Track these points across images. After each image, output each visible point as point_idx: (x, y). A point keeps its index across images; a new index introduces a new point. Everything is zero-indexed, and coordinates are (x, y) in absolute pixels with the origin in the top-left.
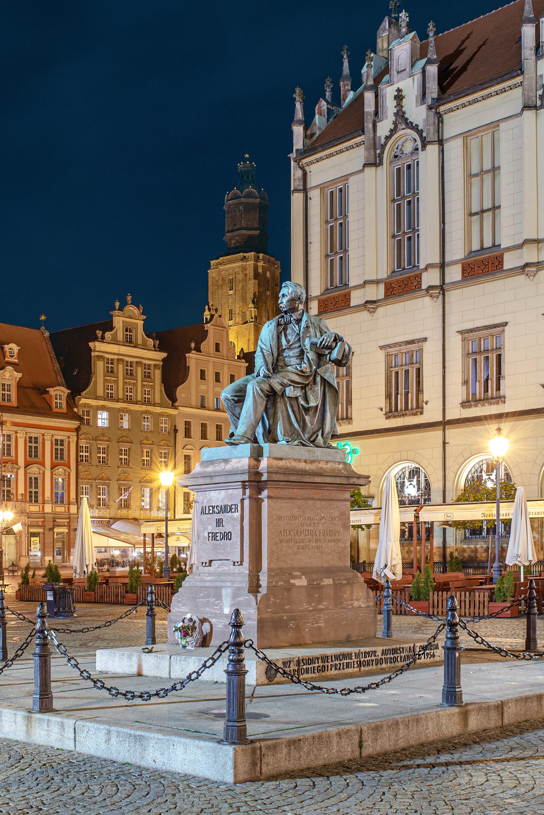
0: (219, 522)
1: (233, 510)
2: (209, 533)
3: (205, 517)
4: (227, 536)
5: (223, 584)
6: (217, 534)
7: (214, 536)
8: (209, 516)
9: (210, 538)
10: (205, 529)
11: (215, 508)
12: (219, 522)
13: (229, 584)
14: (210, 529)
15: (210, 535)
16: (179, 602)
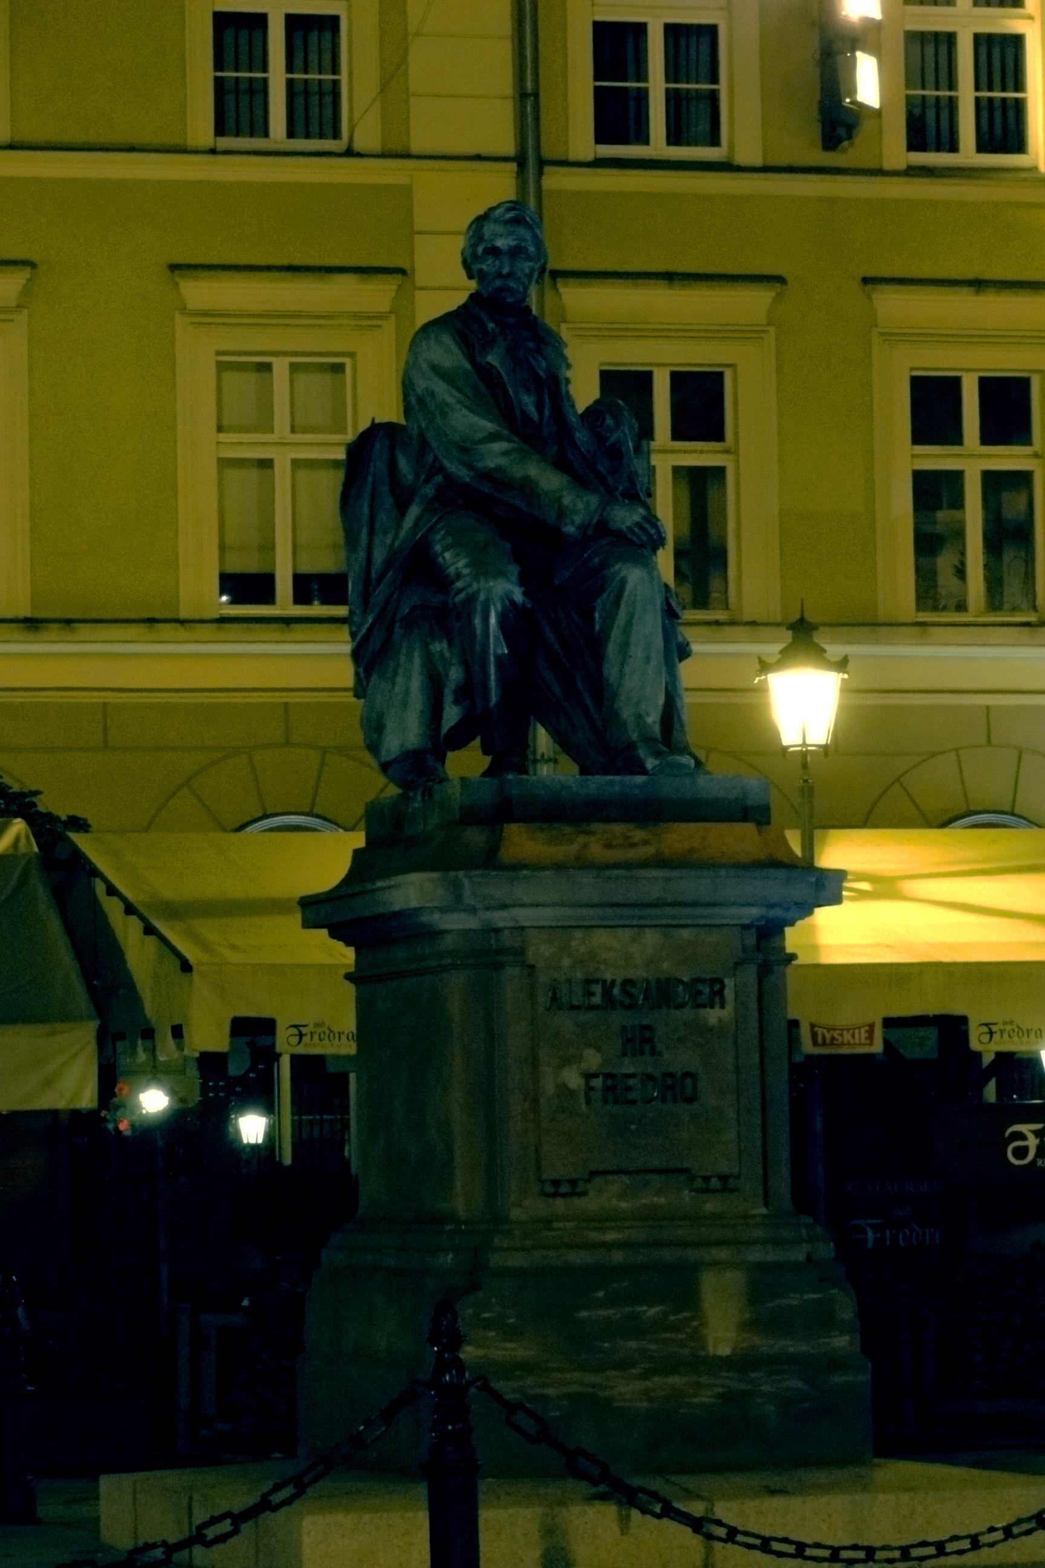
0: (640, 1041)
1: (703, 999)
2: (589, 1076)
3: (565, 1022)
4: (677, 1087)
5: (693, 1255)
6: (631, 1082)
7: (615, 1088)
8: (583, 1016)
9: (596, 1096)
10: (566, 1061)
11: (616, 991)
12: (640, 1041)
13: (722, 1254)
14: (592, 1060)
15: (597, 1083)
16: (487, 1325)
